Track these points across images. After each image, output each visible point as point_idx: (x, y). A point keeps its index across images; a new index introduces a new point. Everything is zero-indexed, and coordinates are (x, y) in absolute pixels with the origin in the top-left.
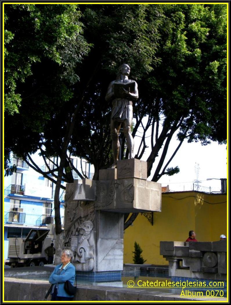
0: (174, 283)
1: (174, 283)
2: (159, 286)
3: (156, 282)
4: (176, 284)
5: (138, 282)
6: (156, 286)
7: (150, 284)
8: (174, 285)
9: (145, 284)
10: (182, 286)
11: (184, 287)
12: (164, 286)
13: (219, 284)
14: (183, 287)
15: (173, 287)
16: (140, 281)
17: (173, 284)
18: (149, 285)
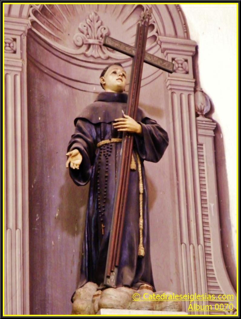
0: (181, 296)
1: (181, 296)
2: (166, 299)
3: (163, 294)
4: (184, 297)
5: (144, 295)
6: (163, 300)
7: (157, 297)
8: (181, 298)
9: (152, 297)
10: (190, 299)
11: (192, 300)
12: (171, 299)
13: (229, 297)
14: (191, 301)
15: (180, 300)
16: (146, 294)
17: (180, 297)
18: (156, 298)
